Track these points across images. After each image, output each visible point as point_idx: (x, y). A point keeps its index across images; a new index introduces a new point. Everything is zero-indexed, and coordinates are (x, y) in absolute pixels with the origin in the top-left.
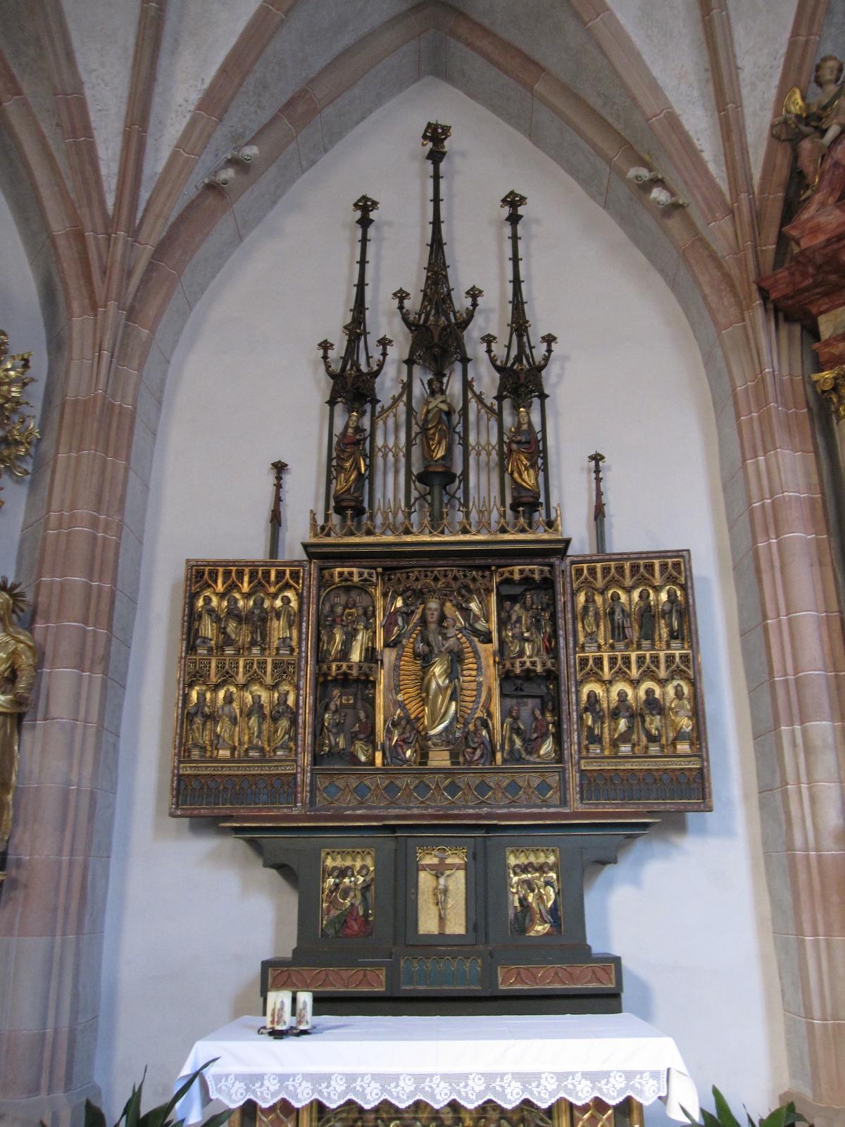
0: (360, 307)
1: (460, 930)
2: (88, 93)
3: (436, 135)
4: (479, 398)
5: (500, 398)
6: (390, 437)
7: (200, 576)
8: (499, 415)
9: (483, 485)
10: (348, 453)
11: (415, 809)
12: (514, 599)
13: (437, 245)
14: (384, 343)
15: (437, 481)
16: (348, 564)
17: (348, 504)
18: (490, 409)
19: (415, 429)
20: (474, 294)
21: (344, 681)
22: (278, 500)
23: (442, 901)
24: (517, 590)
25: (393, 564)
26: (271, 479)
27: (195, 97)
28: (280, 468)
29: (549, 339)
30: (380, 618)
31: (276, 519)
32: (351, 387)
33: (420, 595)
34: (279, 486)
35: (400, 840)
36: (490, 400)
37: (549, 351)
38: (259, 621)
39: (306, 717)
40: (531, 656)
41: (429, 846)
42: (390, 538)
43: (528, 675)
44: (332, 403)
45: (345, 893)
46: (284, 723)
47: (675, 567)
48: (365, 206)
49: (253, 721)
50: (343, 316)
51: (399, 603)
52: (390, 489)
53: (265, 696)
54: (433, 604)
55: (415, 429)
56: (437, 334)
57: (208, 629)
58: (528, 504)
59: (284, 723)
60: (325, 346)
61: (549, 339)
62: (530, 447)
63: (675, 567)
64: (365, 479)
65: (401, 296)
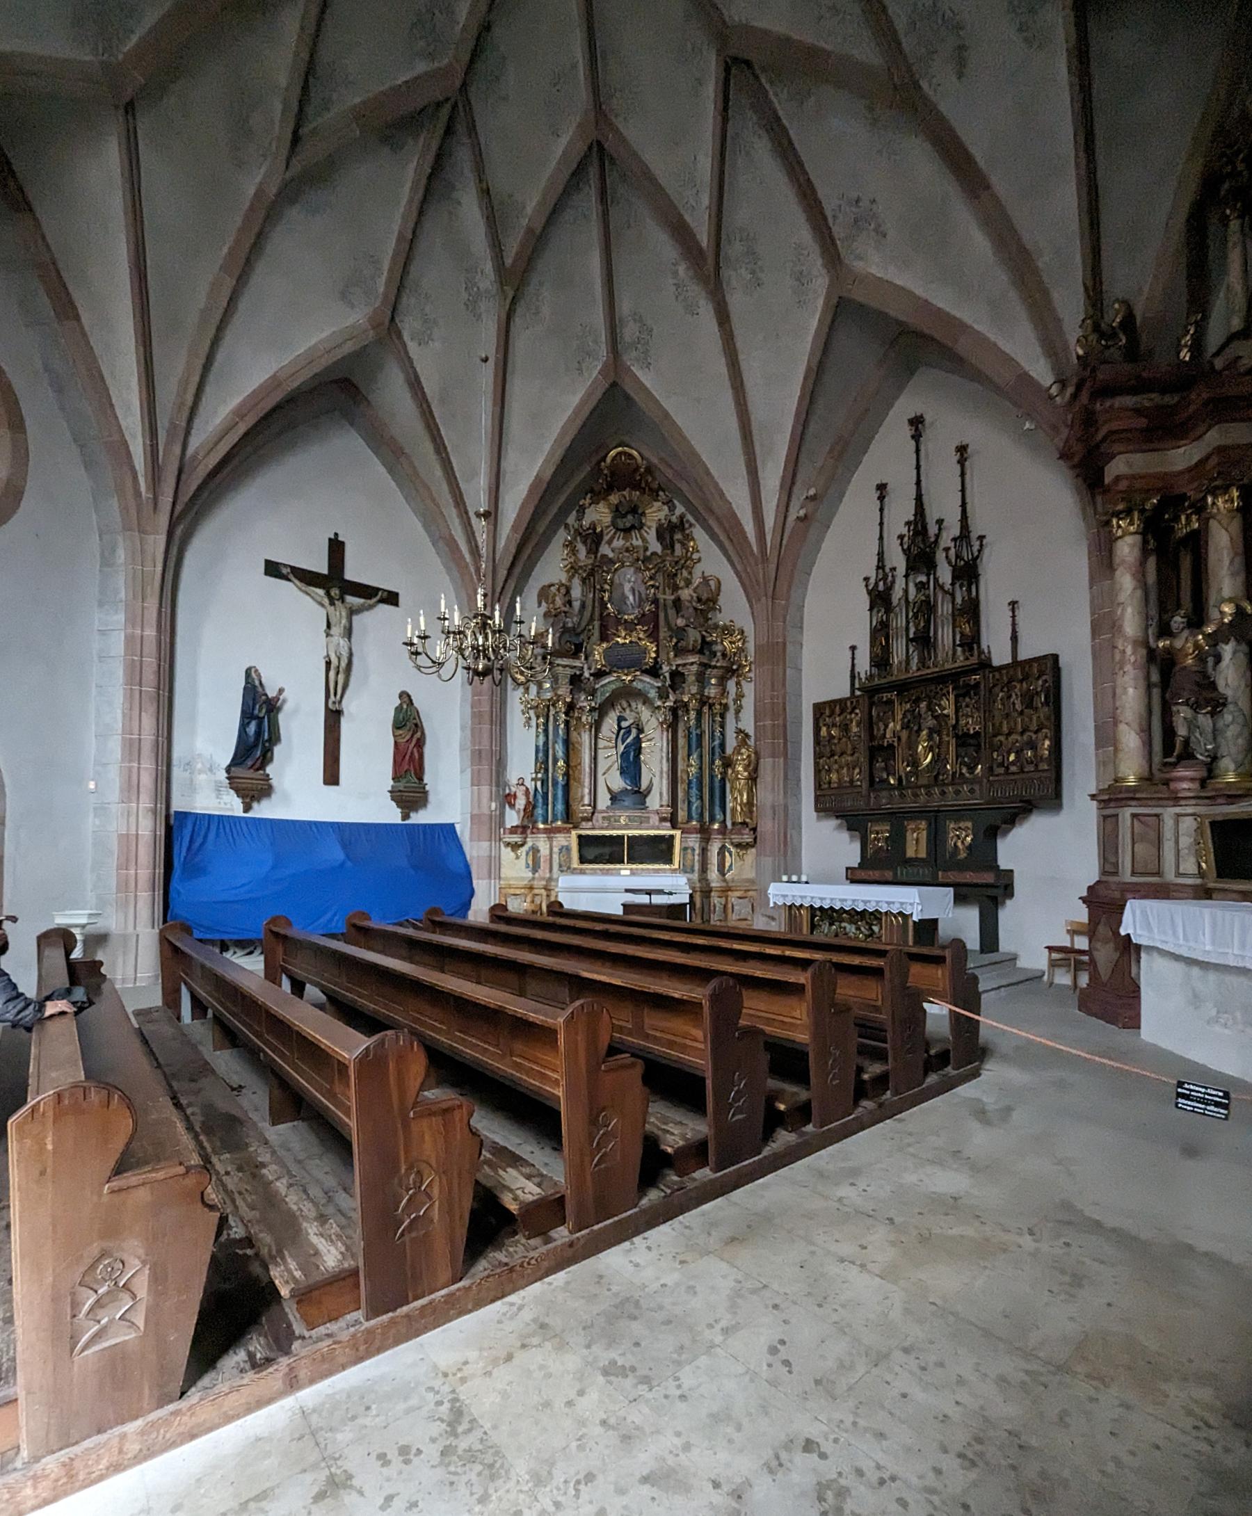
0: (881, 555)
1: (923, 855)
2: (734, 506)
3: (917, 423)
4: (942, 587)
5: (953, 584)
6: (899, 621)
7: (819, 709)
8: (953, 595)
9: (945, 636)
10: (880, 633)
11: (910, 805)
12: (964, 696)
13: (919, 498)
14: (894, 569)
15: (924, 641)
16: (877, 692)
17: (881, 660)
18: (946, 592)
19: (911, 614)
20: (940, 522)
21: (881, 747)
22: (853, 665)
23: (916, 843)
24: (962, 692)
25: (902, 688)
26: (849, 654)
27: (778, 483)
28: (853, 648)
29: (981, 538)
30: (900, 716)
31: (853, 677)
32: (880, 598)
33: (917, 701)
34: (853, 659)
35: (898, 820)
36: (948, 587)
37: (981, 545)
38: (845, 728)
39: (866, 767)
40: (972, 725)
41: (911, 819)
42: (894, 678)
43: (967, 735)
44: (871, 609)
45: (878, 840)
46: (857, 770)
47: (1051, 665)
48: (882, 487)
49: (845, 770)
50: (874, 561)
51: (908, 706)
52: (899, 650)
53: (849, 758)
54: (923, 705)
55: (911, 614)
56: (921, 555)
57: (824, 731)
58: (971, 642)
59: (857, 770)
60: (867, 579)
61: (981, 538)
62: (971, 611)
63: (1051, 665)
64: (887, 650)
65: (901, 537)
